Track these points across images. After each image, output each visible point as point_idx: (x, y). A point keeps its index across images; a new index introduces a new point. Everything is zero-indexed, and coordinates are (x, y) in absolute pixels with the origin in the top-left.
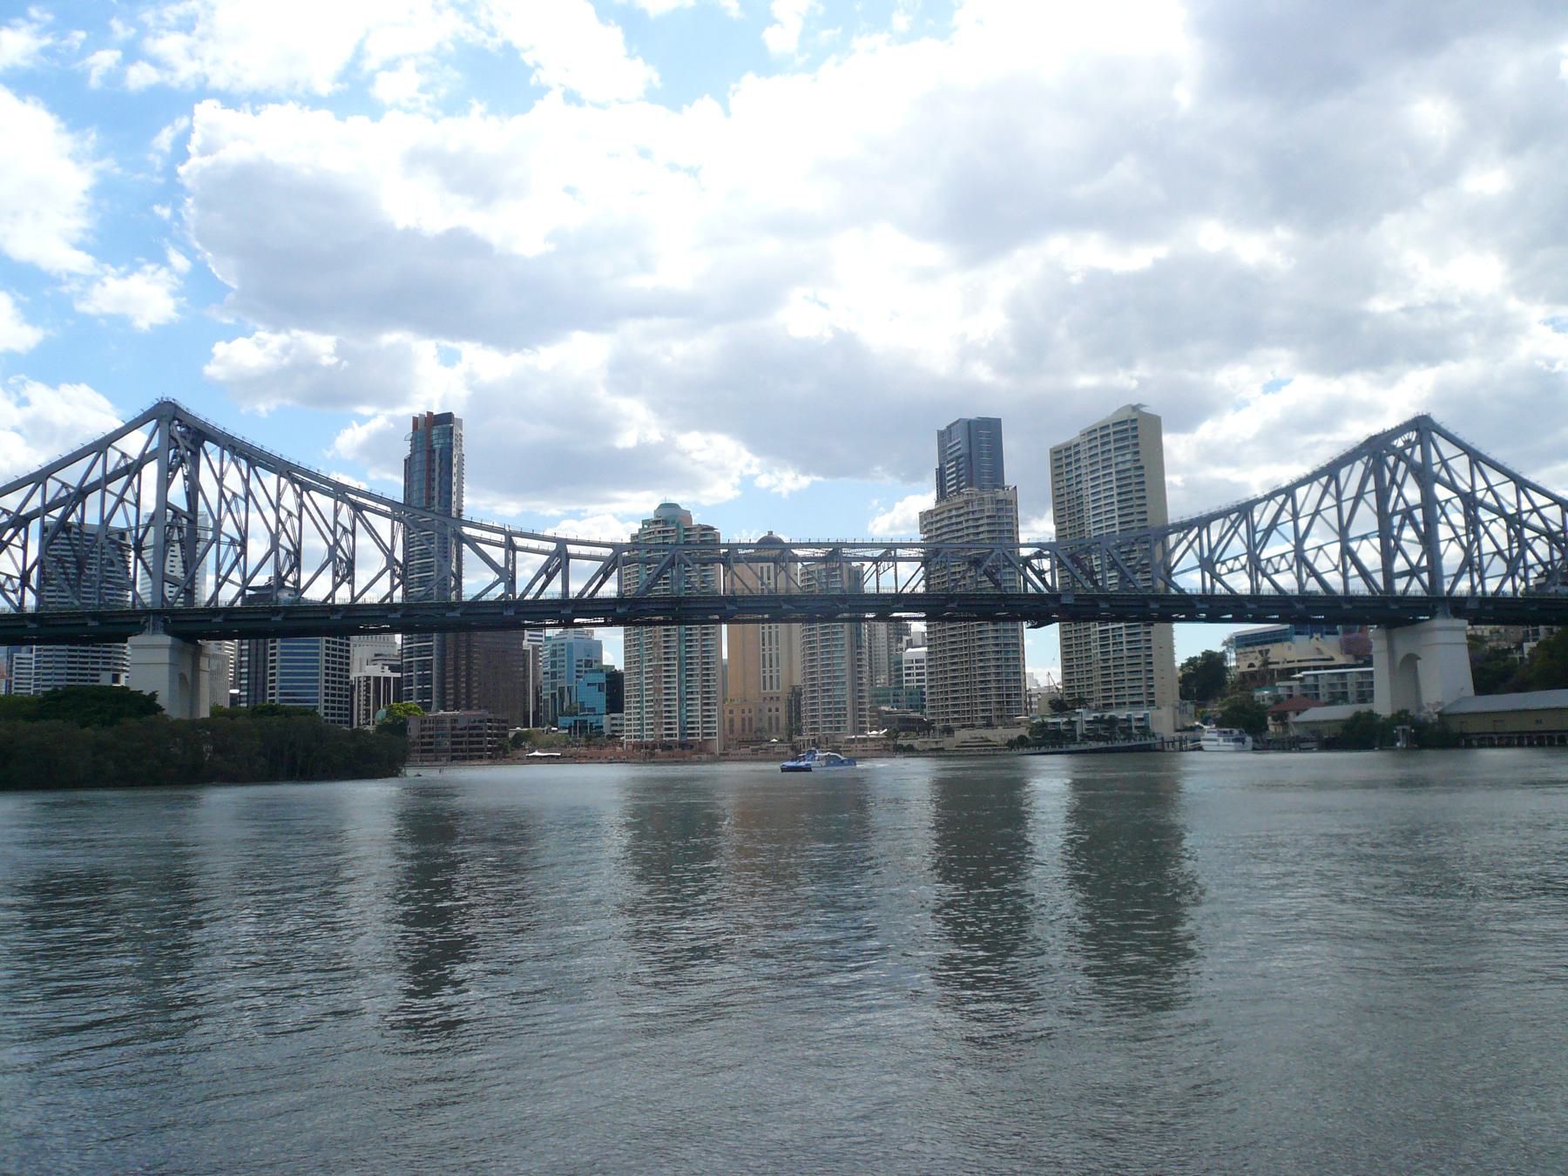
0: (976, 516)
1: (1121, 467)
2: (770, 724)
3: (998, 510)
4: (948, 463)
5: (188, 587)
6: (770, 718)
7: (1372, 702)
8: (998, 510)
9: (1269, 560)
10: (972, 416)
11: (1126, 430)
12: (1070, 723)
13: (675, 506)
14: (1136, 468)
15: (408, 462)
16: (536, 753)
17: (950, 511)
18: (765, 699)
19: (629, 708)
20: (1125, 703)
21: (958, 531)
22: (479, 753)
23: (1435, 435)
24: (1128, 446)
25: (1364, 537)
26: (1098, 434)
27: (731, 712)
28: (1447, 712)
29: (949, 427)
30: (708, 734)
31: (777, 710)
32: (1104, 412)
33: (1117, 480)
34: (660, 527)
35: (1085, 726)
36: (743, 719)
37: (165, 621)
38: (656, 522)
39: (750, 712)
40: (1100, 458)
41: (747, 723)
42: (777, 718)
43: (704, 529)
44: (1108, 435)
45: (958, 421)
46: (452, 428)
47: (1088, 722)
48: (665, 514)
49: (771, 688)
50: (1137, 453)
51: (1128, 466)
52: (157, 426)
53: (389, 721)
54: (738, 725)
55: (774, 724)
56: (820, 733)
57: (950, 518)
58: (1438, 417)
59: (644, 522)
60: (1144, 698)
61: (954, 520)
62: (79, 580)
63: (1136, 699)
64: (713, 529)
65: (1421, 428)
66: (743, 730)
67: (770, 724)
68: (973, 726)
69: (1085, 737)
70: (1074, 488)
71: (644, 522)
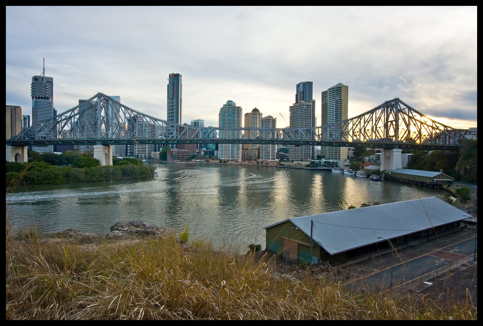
1: (337, 99)
2: (254, 155)
3: (308, 107)
4: (299, 93)
5: (107, 133)
6: (254, 154)
8: (308, 107)
9: (355, 132)
10: (305, 81)
11: (338, 90)
12: (320, 162)
13: (232, 101)
14: (340, 100)
15: (168, 85)
16: (197, 160)
17: (296, 107)
19: (219, 150)
20: (333, 158)
21: (298, 112)
22: (184, 160)
24: (338, 94)
26: (332, 90)
27: (245, 152)
28: (393, 172)
29: (299, 84)
32: (334, 84)
33: (335, 102)
34: (228, 107)
36: (247, 154)
37: (101, 142)
38: (227, 105)
39: (249, 152)
41: (248, 155)
42: (255, 154)
43: (238, 107)
45: (301, 83)
47: (324, 162)
48: (230, 103)
49: (254, 147)
51: (338, 99)
52: (98, 98)
53: (163, 151)
55: (254, 155)
56: (264, 159)
57: (296, 109)
58: (401, 99)
59: (224, 105)
60: (338, 157)
61: (297, 109)
63: (336, 157)
64: (240, 107)
66: (247, 156)
67: (254, 155)
68: (298, 160)
69: (323, 166)
71: (224, 105)
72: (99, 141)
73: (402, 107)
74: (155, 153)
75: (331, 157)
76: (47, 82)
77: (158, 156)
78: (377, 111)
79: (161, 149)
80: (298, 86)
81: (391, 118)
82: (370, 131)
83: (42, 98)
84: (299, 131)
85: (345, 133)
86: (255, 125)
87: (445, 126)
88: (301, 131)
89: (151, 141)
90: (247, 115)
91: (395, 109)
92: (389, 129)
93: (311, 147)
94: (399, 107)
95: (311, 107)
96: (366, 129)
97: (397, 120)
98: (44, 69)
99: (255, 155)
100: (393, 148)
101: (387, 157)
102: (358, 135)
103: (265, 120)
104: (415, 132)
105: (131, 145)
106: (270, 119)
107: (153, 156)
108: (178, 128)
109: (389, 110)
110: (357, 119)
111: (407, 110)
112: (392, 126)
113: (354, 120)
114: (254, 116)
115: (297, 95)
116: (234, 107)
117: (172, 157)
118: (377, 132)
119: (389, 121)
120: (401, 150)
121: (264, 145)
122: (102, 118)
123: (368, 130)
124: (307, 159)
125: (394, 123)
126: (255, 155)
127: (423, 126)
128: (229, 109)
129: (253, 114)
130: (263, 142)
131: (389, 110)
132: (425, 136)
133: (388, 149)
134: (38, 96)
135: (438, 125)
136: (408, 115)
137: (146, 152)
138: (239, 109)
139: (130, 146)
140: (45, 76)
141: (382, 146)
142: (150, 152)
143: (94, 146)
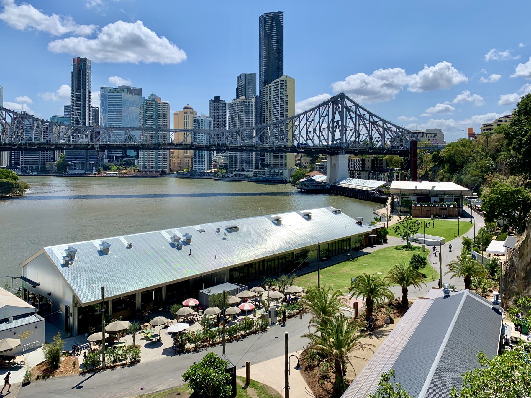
10: (247, 73)
15: (72, 74)
25: (324, 129)
26: (276, 84)
30: (165, 168)
34: (150, 102)
36: (178, 163)
38: (149, 101)
42: (188, 163)
44: (278, 84)
46: (86, 63)
48: (152, 98)
54: (176, 164)
80: (239, 78)
82: (312, 133)
87: (398, 127)
89: (35, 145)
95: (253, 105)
96: (308, 131)
103: (198, 120)
105: (16, 152)
112: (337, 127)
114: (186, 115)
115: (237, 89)
116: (160, 103)
119: (335, 120)
121: (197, 152)
125: (340, 122)
127: (374, 127)
128: (151, 106)
129: (185, 113)
130: (177, 147)
132: (375, 138)
133: (334, 155)
138: (165, 106)
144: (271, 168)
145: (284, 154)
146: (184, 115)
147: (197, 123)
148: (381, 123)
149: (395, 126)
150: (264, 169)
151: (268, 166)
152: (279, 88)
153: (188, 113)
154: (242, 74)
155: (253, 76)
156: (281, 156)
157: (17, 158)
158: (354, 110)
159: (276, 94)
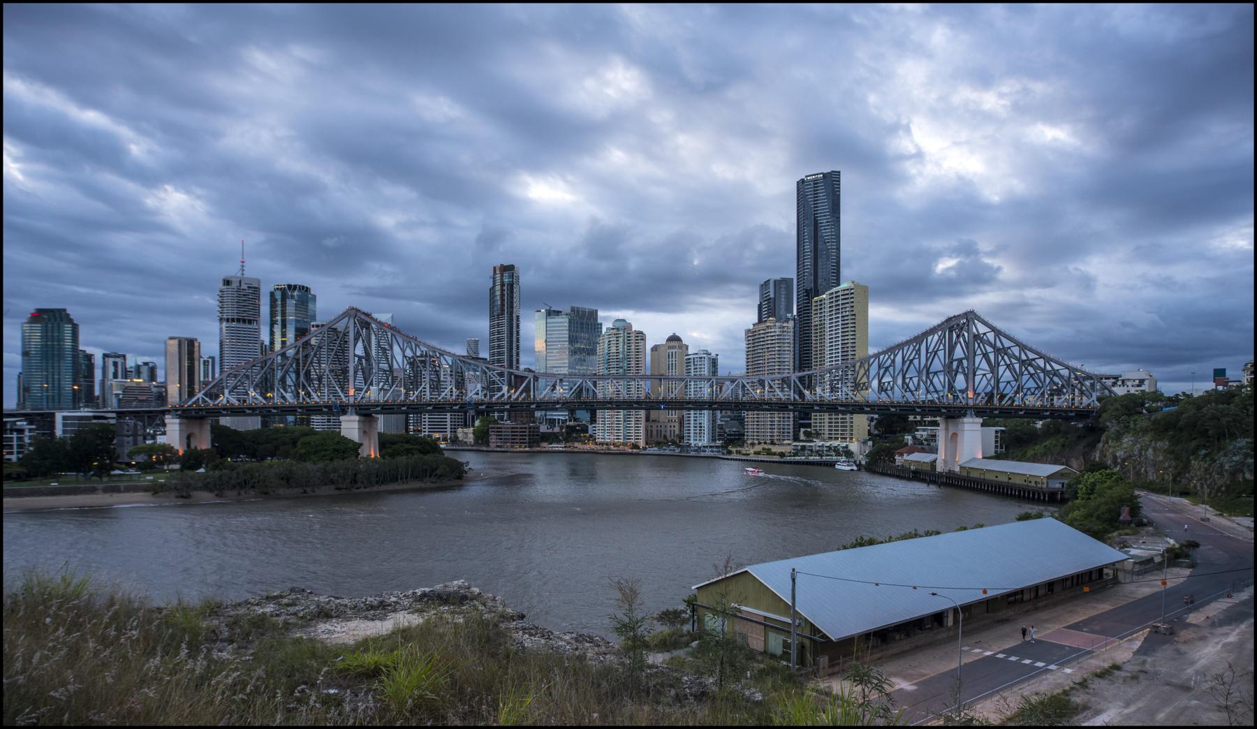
0: (773, 334)
1: (844, 314)
2: (671, 433)
4: (764, 301)
6: (671, 431)
7: (937, 453)
18: (669, 421)
19: (599, 424)
23: (976, 321)
26: (834, 295)
27: (651, 426)
29: (765, 282)
31: (674, 427)
34: (615, 331)
35: (818, 448)
36: (657, 431)
37: (356, 409)
40: (834, 308)
42: (674, 431)
47: (819, 446)
48: (619, 325)
50: (852, 307)
55: (672, 434)
57: (760, 334)
62: (320, 387)
65: (969, 318)
66: (657, 436)
67: (671, 433)
70: (823, 322)
72: (352, 406)
73: (982, 329)
74: (466, 430)
75: (833, 436)
76: (249, 287)
77: (472, 436)
78: (930, 338)
79: (477, 423)
81: (959, 352)
82: (916, 380)
83: (238, 320)
84: (766, 382)
85: (862, 385)
86: (672, 369)
88: (770, 382)
90: (655, 349)
91: (966, 334)
92: (956, 375)
93: (791, 415)
94: (975, 330)
97: (970, 356)
98: (243, 262)
99: (674, 433)
100: (965, 415)
101: (950, 434)
102: (889, 388)
103: (694, 358)
104: (1009, 382)
105: (415, 415)
106: (704, 358)
107: (460, 436)
108: (513, 377)
109: (955, 336)
110: (887, 356)
111: (991, 336)
112: (960, 370)
113: (882, 357)
114: (670, 351)
115: (760, 307)
117: (501, 439)
118: (929, 382)
120: (981, 420)
121: (692, 412)
122: (356, 359)
123: (911, 378)
124: (784, 440)
125: (965, 362)
126: (674, 433)
127: (1026, 369)
128: (617, 337)
129: (670, 348)
131: (955, 336)
132: (1029, 389)
133: (953, 417)
134: (230, 317)
135: (1056, 367)
136: (993, 346)
137: (446, 428)
138: (641, 336)
139: (414, 417)
140: (245, 276)
141: (940, 410)
142: (455, 428)
143: (342, 418)
144: (824, 440)
145: (848, 416)
146: (668, 351)
147: (692, 364)
148: (1041, 362)
149: (1067, 367)
150: (812, 441)
151: (818, 435)
152: (840, 302)
153: (674, 347)
154: (769, 280)
155: (786, 282)
156: (842, 419)
157: (417, 423)
158: (992, 340)
159: (834, 312)
